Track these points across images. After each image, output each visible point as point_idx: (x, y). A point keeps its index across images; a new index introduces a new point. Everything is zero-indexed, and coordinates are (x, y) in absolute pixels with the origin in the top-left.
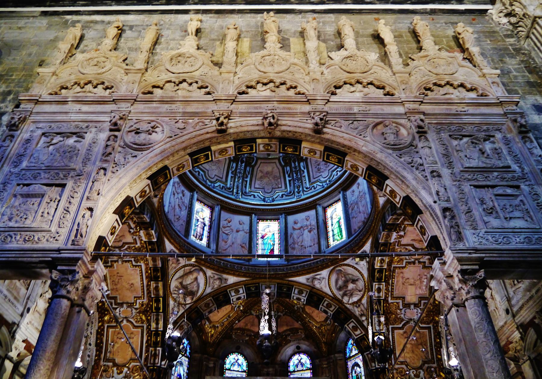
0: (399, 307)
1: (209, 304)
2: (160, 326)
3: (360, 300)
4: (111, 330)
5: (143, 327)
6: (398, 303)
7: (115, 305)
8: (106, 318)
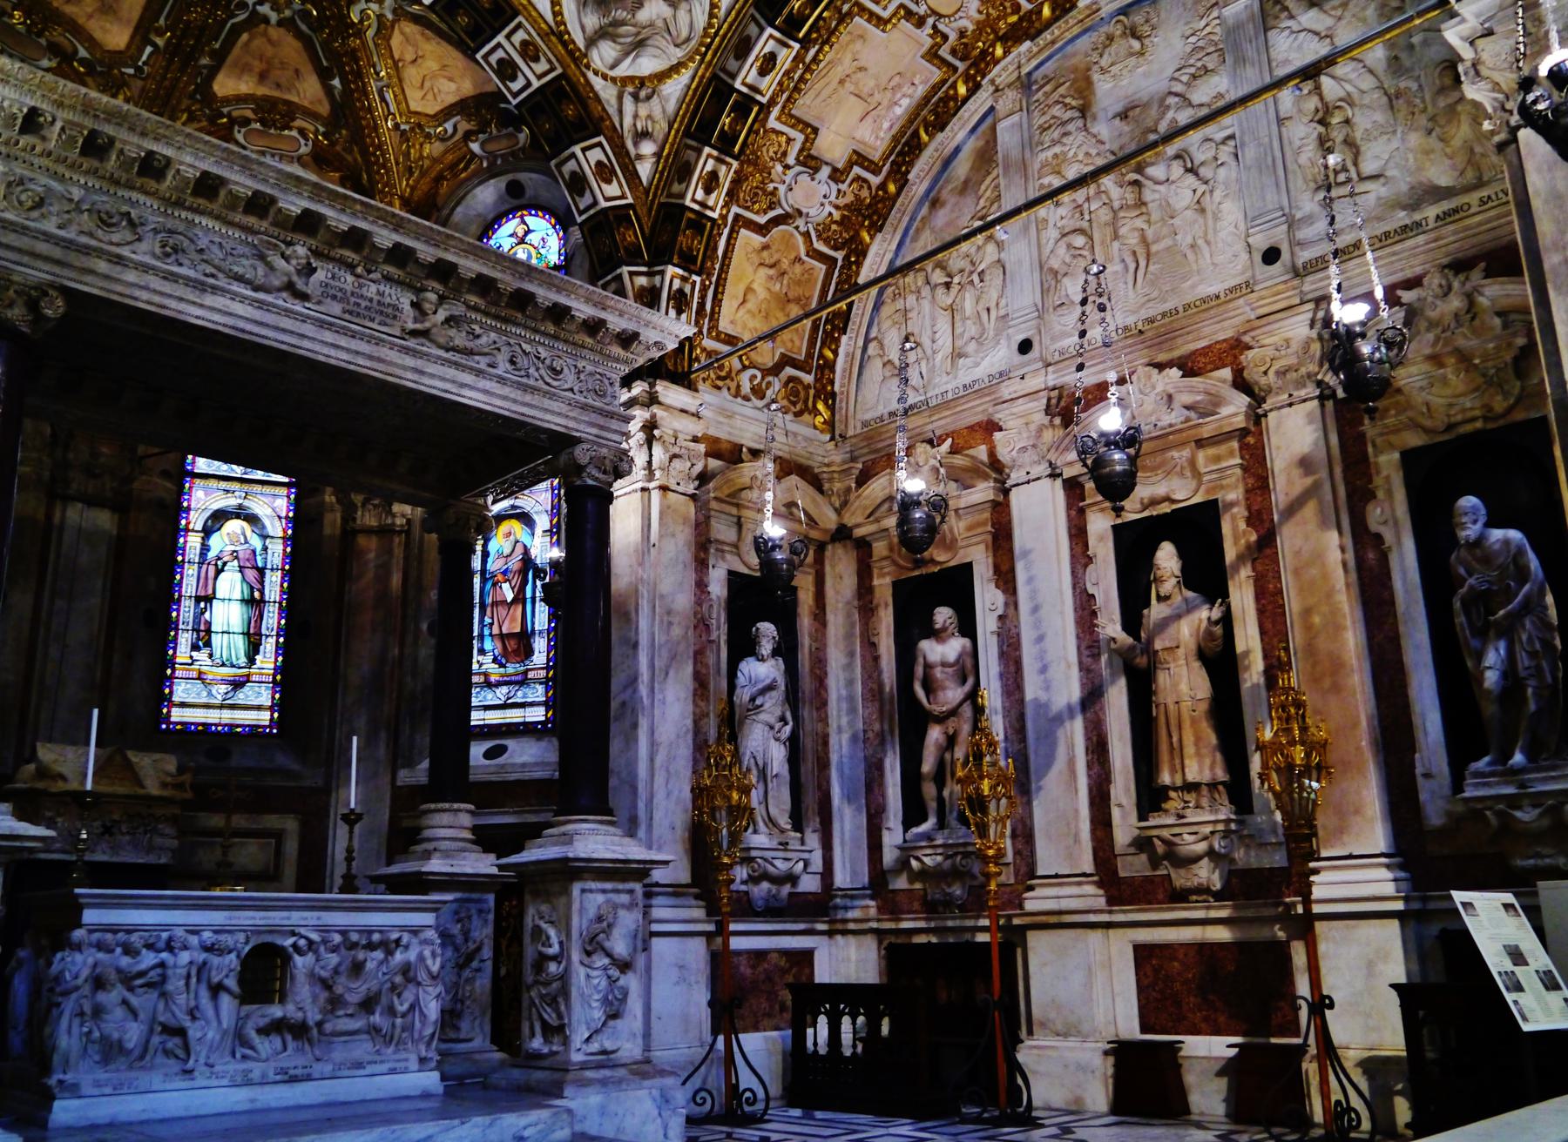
0: (785, 154)
3: (662, 77)
6: (789, 140)
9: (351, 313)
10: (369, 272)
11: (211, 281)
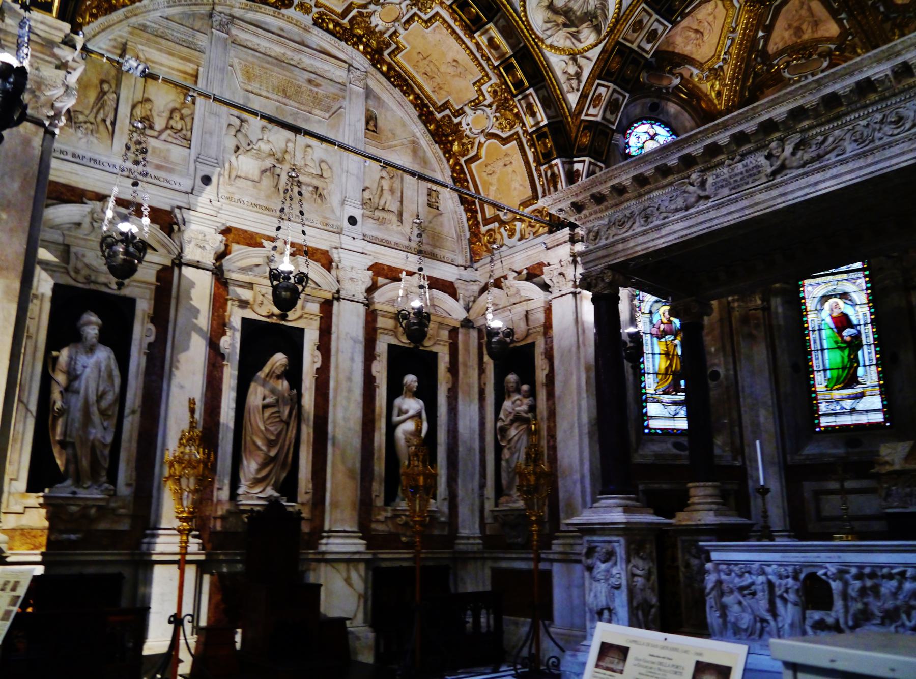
1: (641, 21)
2: (540, 119)
4: (473, 166)
5: (517, 133)
7: (456, 117)
8: (456, 147)
9: (734, 188)
10: (733, 159)
11: (666, 220)
